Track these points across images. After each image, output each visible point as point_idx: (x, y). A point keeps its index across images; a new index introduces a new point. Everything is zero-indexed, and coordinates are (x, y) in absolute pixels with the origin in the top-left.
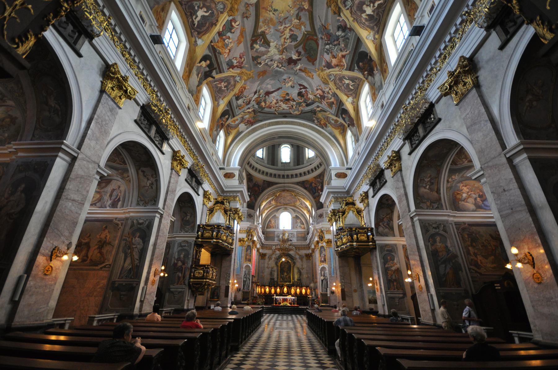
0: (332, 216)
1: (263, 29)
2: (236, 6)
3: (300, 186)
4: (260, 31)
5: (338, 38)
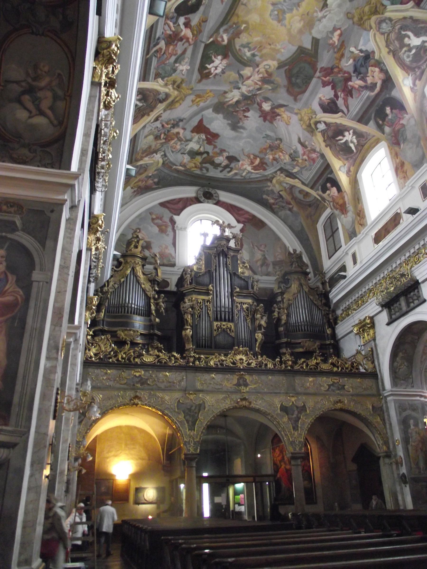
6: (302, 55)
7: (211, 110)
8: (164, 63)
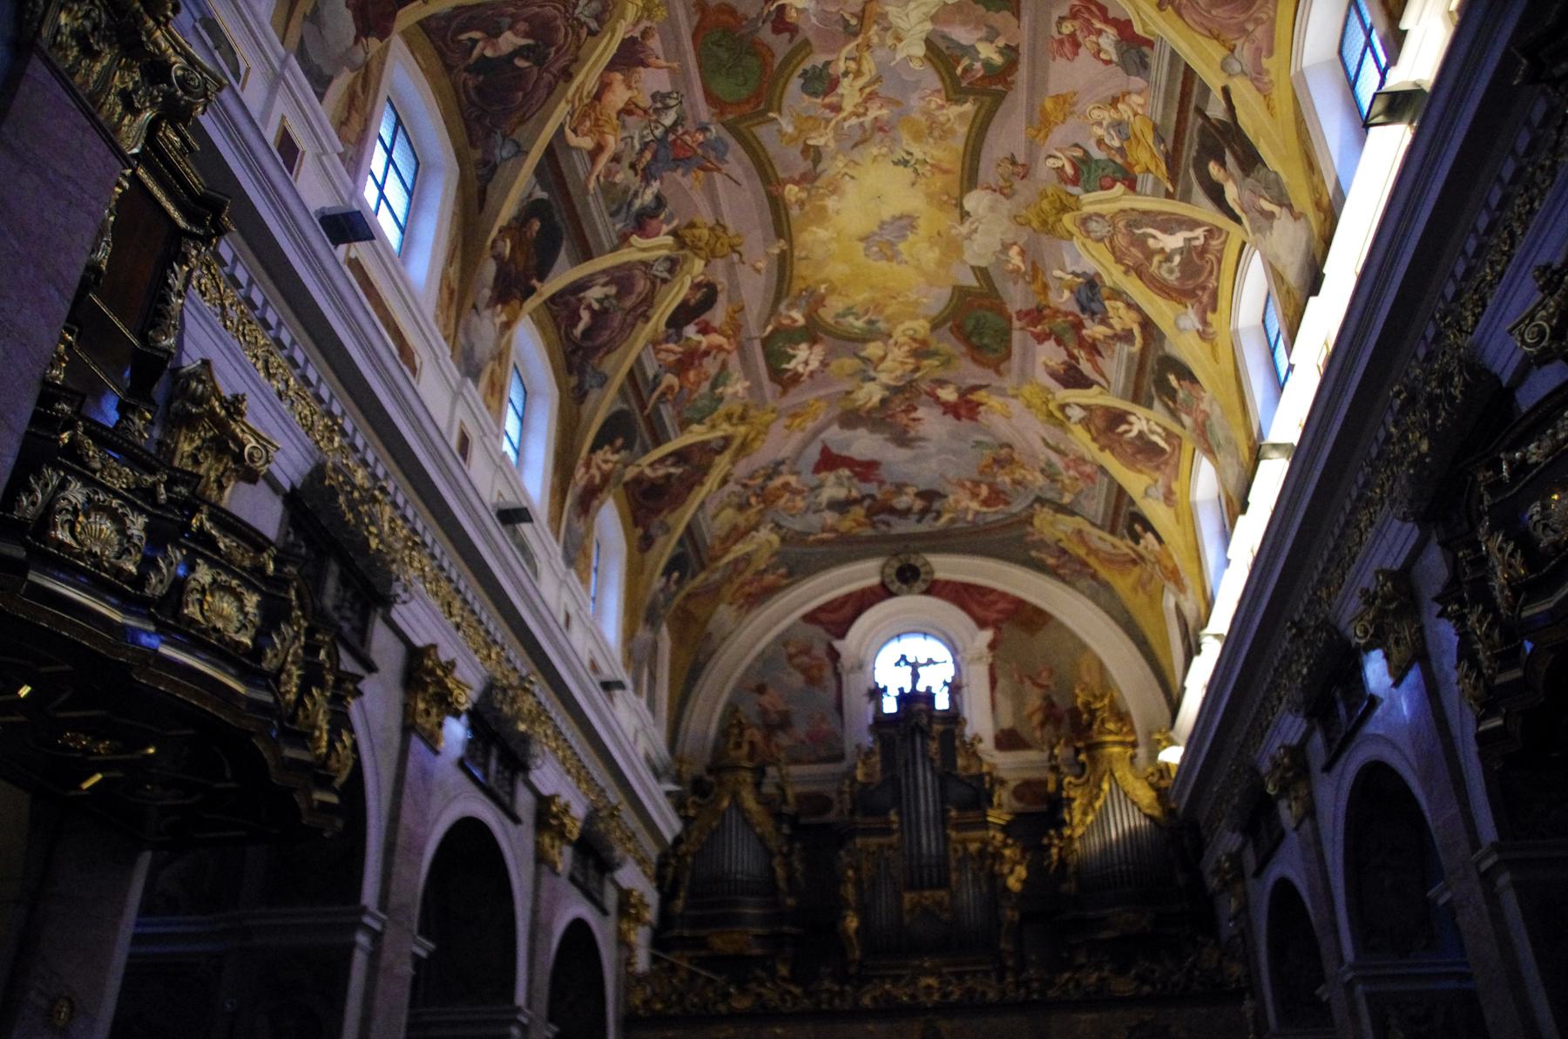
1: (954, 111)
2: (1045, 205)
4: (968, 107)
5: (647, 176)
6: (969, 299)
7: (835, 428)
8: (688, 401)
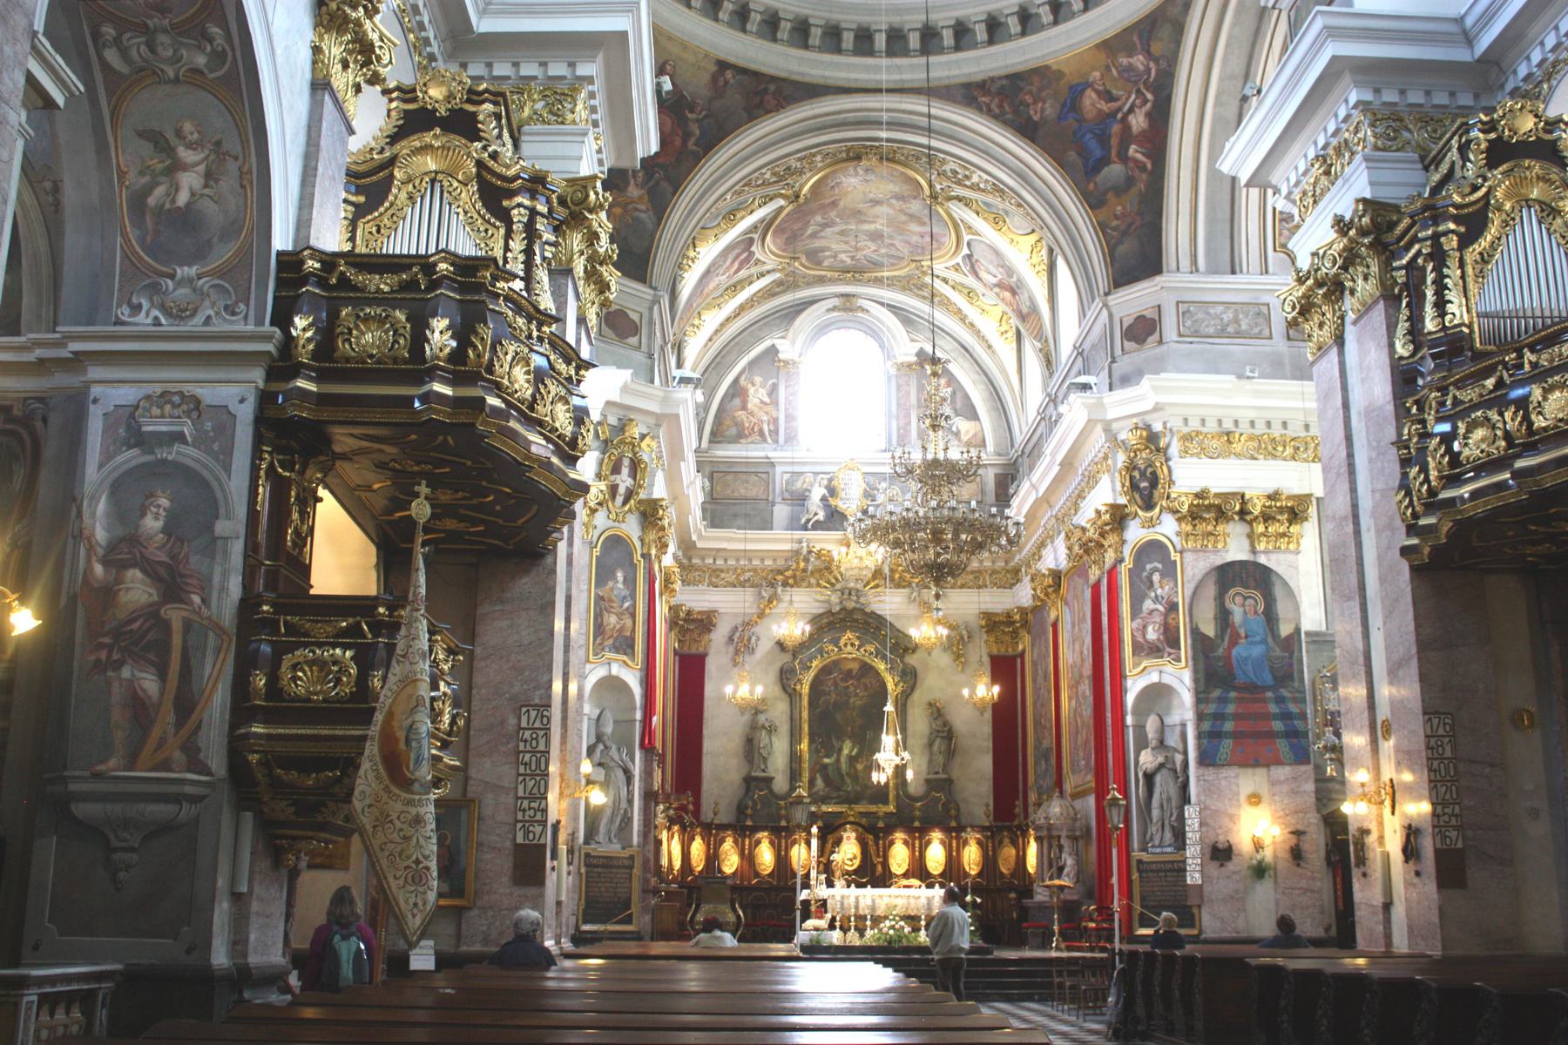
0: (1350, 259)
3: (987, 111)
